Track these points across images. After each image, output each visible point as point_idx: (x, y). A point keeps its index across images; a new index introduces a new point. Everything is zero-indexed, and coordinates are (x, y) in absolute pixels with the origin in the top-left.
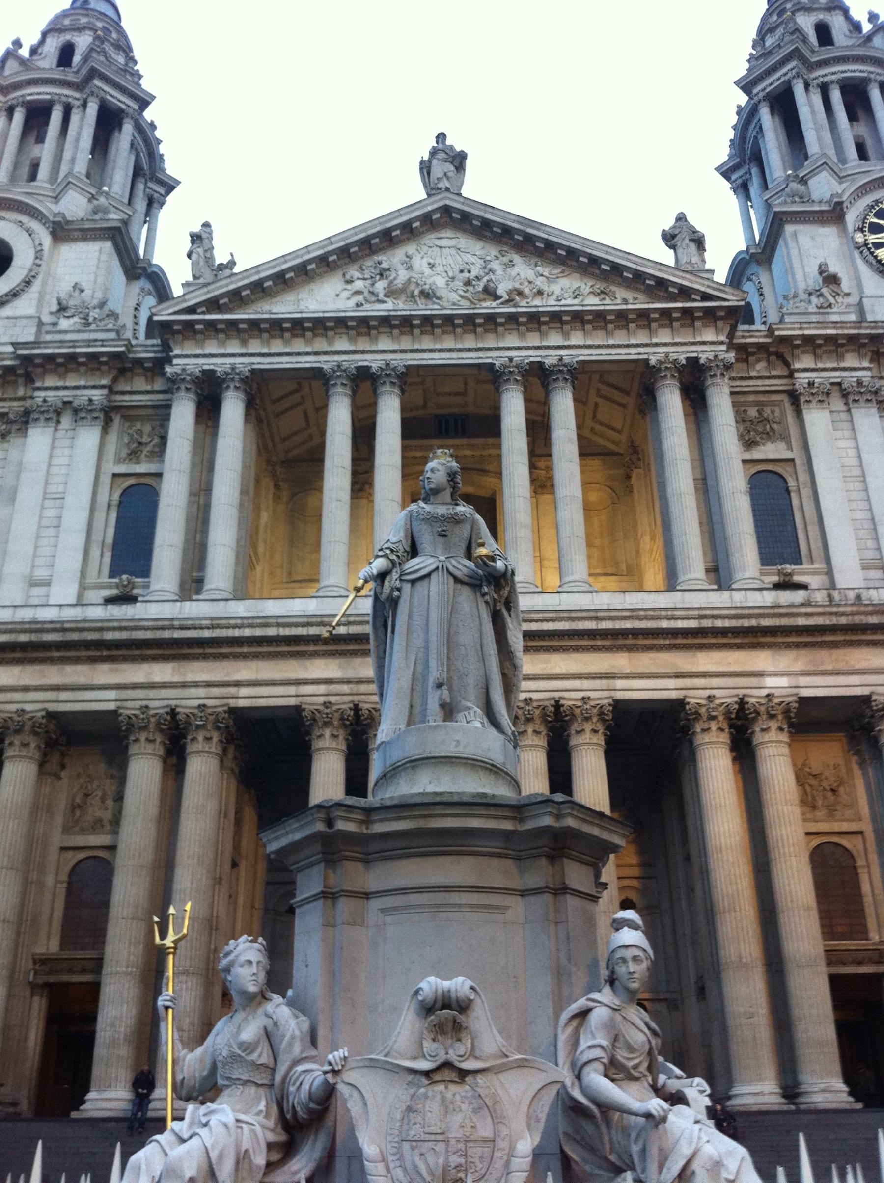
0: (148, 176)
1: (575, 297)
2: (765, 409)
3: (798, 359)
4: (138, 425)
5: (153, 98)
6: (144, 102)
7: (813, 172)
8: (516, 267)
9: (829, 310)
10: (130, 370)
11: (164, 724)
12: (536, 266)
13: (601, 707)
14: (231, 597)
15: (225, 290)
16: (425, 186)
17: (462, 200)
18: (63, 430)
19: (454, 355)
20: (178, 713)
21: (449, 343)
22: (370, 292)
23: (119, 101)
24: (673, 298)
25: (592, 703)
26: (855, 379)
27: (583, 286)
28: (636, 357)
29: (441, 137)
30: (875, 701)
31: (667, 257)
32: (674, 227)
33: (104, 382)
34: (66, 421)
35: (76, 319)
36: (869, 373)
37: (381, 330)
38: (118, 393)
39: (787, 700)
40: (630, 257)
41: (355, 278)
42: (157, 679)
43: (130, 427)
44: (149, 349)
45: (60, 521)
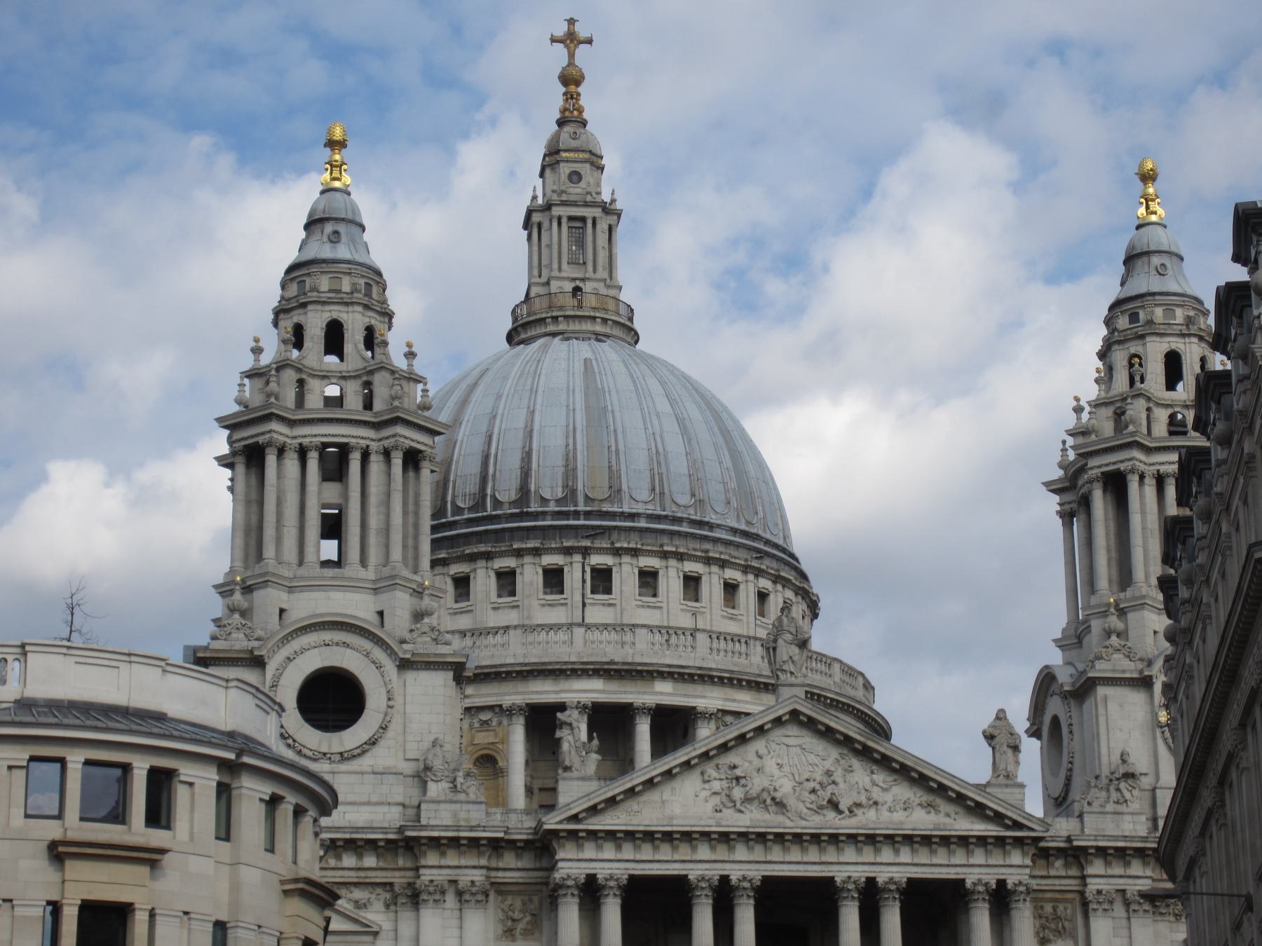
1: (905, 809)
2: (1059, 904)
3: (1091, 862)
4: (509, 900)
8: (855, 774)
9: (1123, 808)
10: (502, 847)
12: (872, 773)
18: (448, 909)
19: (801, 867)
21: (795, 854)
22: (728, 796)
23: (419, 442)
24: (987, 819)
27: (912, 798)
33: (483, 862)
36: (1149, 882)
41: (712, 777)
43: (503, 902)
44: (523, 831)
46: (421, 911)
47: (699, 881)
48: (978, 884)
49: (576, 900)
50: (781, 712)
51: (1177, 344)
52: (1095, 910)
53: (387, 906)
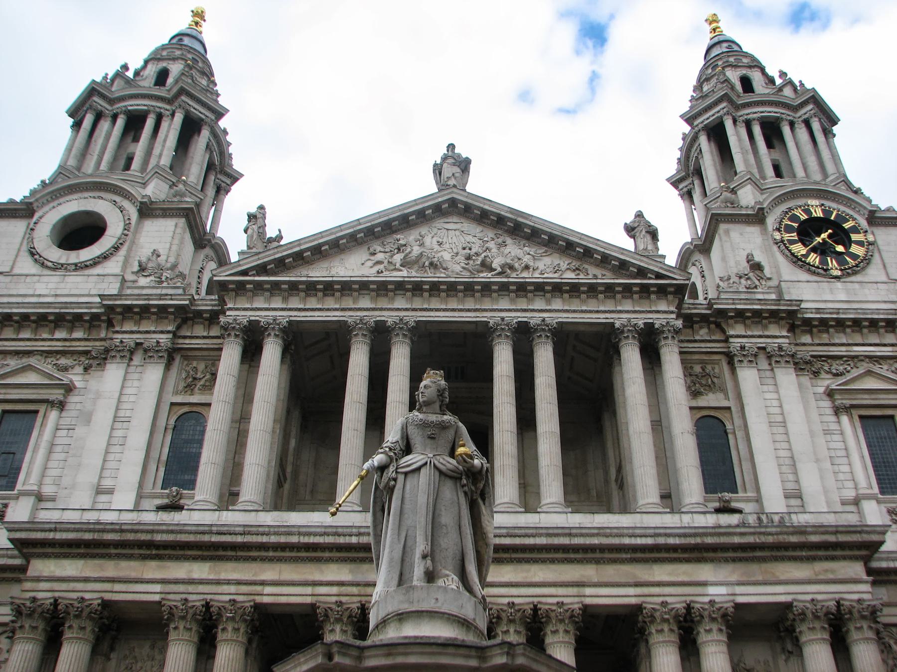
0: (218, 169)
1: (556, 272)
2: (707, 366)
3: (733, 328)
4: (195, 364)
5: (227, 111)
6: (220, 114)
7: (741, 185)
9: (755, 290)
10: (192, 319)
11: (200, 615)
13: (573, 611)
14: (261, 508)
15: (272, 258)
16: (437, 183)
17: (466, 194)
19: (456, 314)
20: (212, 606)
22: (389, 262)
23: (200, 112)
25: (566, 607)
26: (776, 345)
28: (604, 321)
29: (451, 147)
30: (796, 607)
31: (628, 244)
32: (634, 222)
33: (170, 328)
34: (137, 359)
35: (152, 278)
36: (787, 341)
37: (398, 292)
38: (180, 337)
39: (726, 605)
40: (599, 243)
41: (378, 251)
42: (196, 575)
44: (208, 302)
45: (125, 440)
46: (108, 366)
47: (357, 324)
48: (627, 326)
49: (239, 340)
50: (440, 200)
51: (744, 71)
52: (741, 361)
53: (86, 369)
